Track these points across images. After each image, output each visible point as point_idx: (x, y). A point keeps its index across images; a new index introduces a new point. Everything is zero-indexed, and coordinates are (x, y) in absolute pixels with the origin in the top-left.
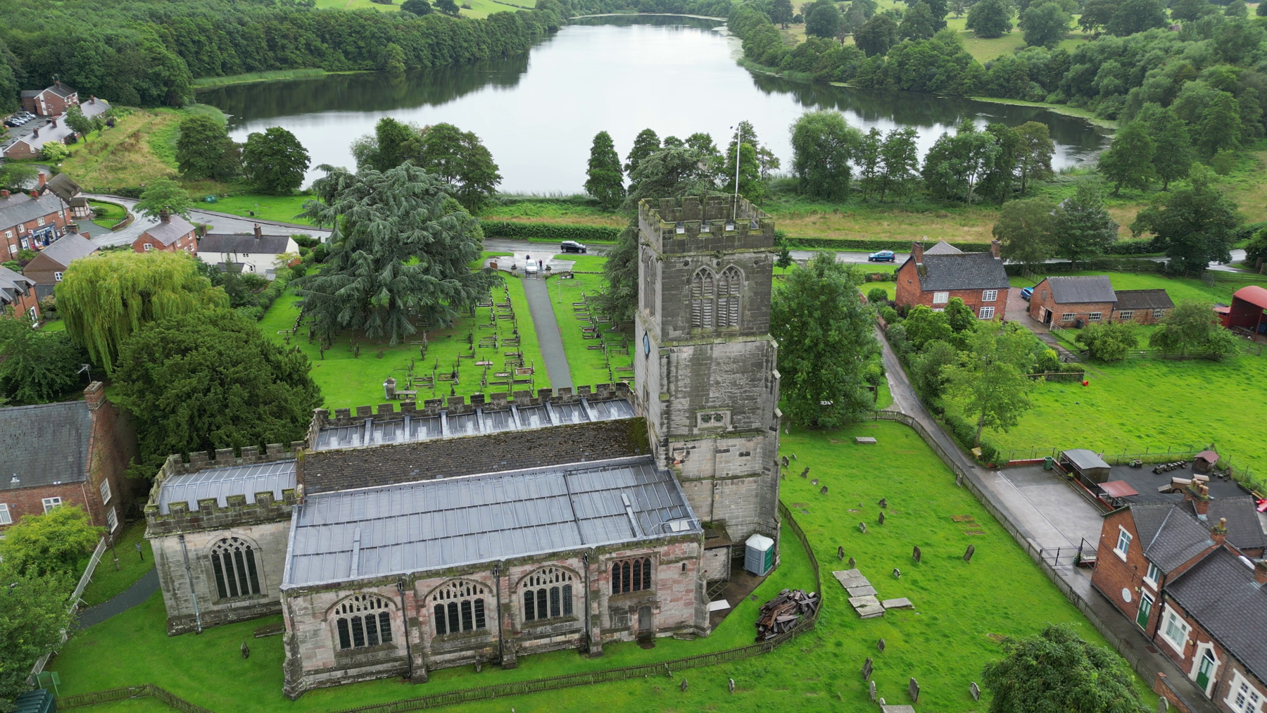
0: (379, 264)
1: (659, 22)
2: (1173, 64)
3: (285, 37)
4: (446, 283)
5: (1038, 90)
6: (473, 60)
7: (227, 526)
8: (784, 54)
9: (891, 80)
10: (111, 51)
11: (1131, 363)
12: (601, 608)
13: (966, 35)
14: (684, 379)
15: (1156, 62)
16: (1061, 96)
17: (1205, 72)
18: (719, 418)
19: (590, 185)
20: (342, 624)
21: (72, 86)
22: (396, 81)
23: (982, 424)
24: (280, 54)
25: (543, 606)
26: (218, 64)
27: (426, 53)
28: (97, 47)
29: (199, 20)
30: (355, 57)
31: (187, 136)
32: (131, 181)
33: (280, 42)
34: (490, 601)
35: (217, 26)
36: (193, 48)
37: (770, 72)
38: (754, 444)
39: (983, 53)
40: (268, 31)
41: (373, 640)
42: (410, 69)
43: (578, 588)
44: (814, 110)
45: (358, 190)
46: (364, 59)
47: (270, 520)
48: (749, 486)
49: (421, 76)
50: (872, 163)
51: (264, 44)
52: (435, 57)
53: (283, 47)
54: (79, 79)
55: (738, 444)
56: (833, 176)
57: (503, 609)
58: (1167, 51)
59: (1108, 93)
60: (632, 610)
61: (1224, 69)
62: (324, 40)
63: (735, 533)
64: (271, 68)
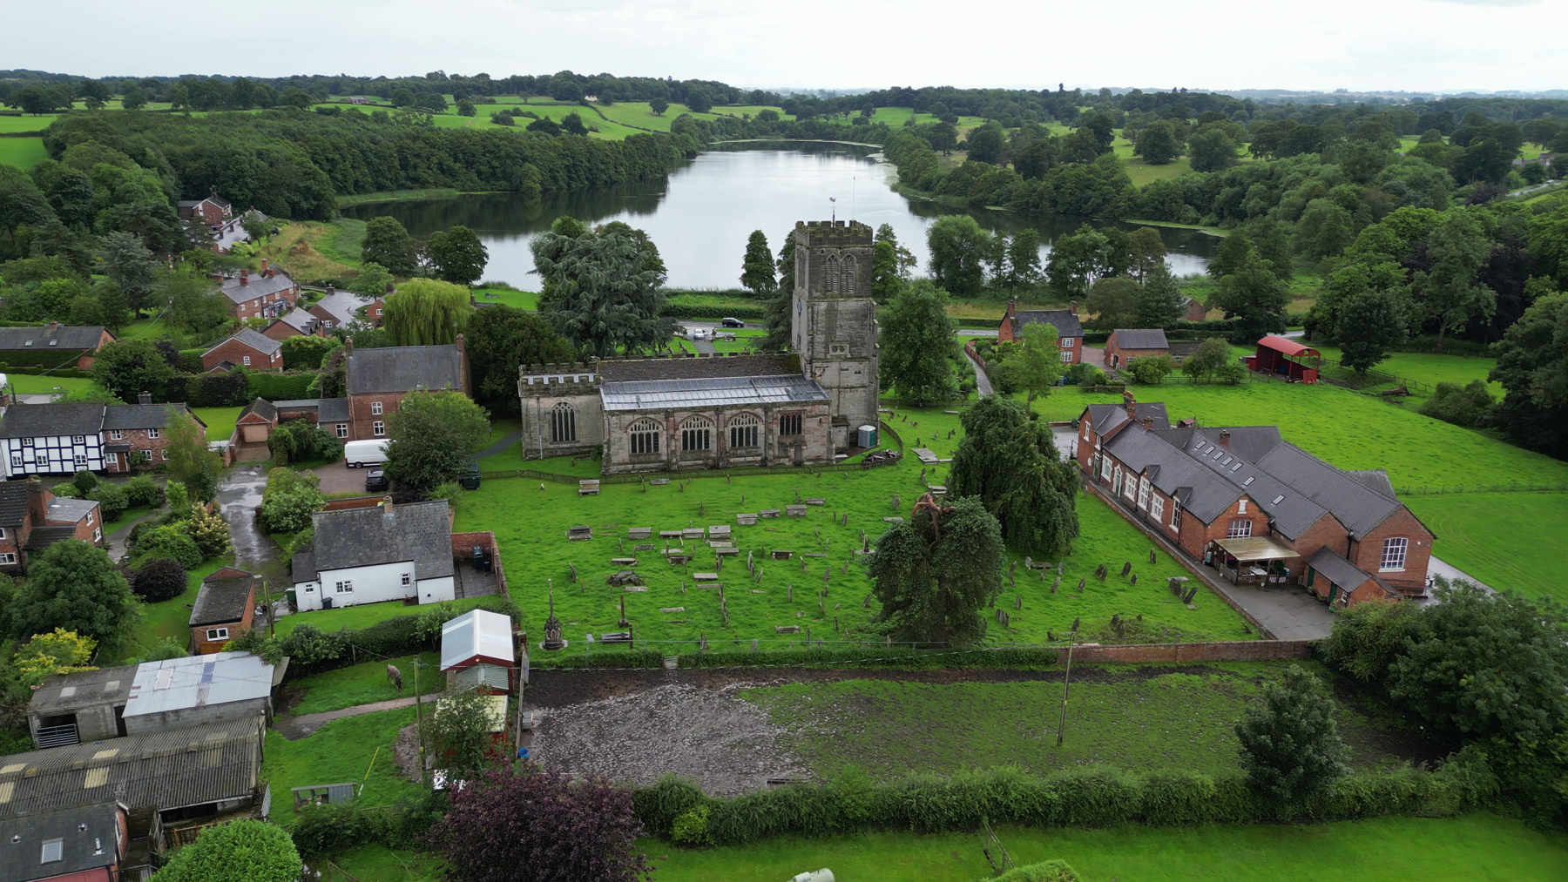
0: (595, 304)
1: (808, 150)
2: (1308, 184)
3: (417, 156)
4: (644, 321)
5: (1192, 213)
6: (611, 183)
7: (563, 395)
8: (940, 178)
9: (1046, 203)
10: (264, 164)
11: (1167, 385)
12: (774, 439)
13: (1132, 162)
14: (822, 324)
15: (1298, 181)
16: (1215, 219)
17: (1332, 191)
18: (842, 349)
19: (746, 279)
20: (634, 436)
21: (226, 197)
22: (531, 202)
23: (1032, 398)
24: (412, 173)
25: (743, 438)
26: (351, 182)
27: (562, 175)
28: (250, 162)
29: (334, 138)
30: (490, 177)
31: (374, 235)
32: (321, 276)
33: (413, 161)
34: (713, 430)
35: (351, 145)
36: (328, 167)
37: (925, 197)
38: (864, 366)
39: (1142, 178)
40: (401, 150)
41: (649, 450)
42: (545, 191)
43: (761, 428)
44: (946, 218)
45: (578, 252)
46: (498, 179)
47: (587, 393)
48: (861, 393)
49: (556, 198)
50: (999, 264)
51: (397, 163)
52: (571, 178)
53: (415, 167)
54: (232, 191)
55: (854, 365)
56: (965, 275)
57: (720, 435)
58: (1307, 173)
59: (1255, 215)
60: (791, 445)
61: (1346, 188)
62: (456, 160)
63: (854, 424)
64: (402, 187)
